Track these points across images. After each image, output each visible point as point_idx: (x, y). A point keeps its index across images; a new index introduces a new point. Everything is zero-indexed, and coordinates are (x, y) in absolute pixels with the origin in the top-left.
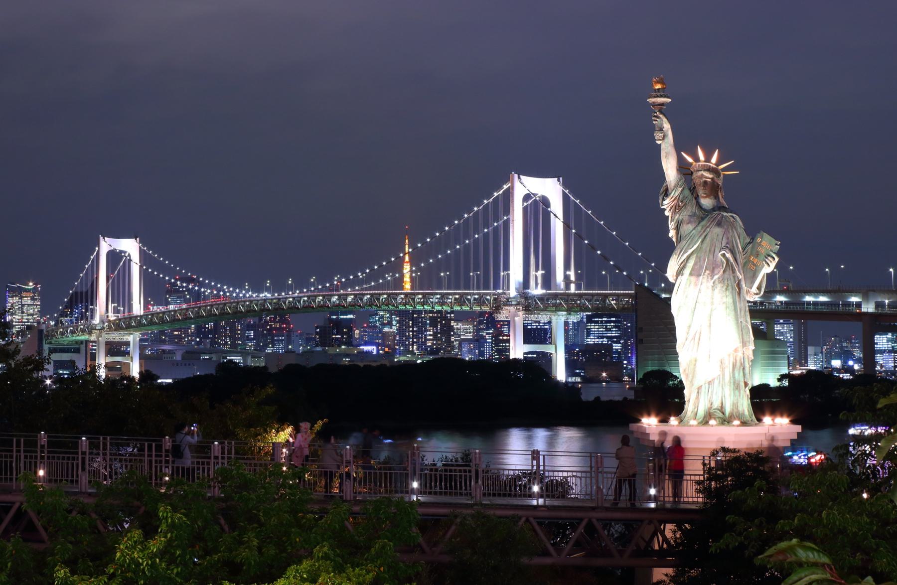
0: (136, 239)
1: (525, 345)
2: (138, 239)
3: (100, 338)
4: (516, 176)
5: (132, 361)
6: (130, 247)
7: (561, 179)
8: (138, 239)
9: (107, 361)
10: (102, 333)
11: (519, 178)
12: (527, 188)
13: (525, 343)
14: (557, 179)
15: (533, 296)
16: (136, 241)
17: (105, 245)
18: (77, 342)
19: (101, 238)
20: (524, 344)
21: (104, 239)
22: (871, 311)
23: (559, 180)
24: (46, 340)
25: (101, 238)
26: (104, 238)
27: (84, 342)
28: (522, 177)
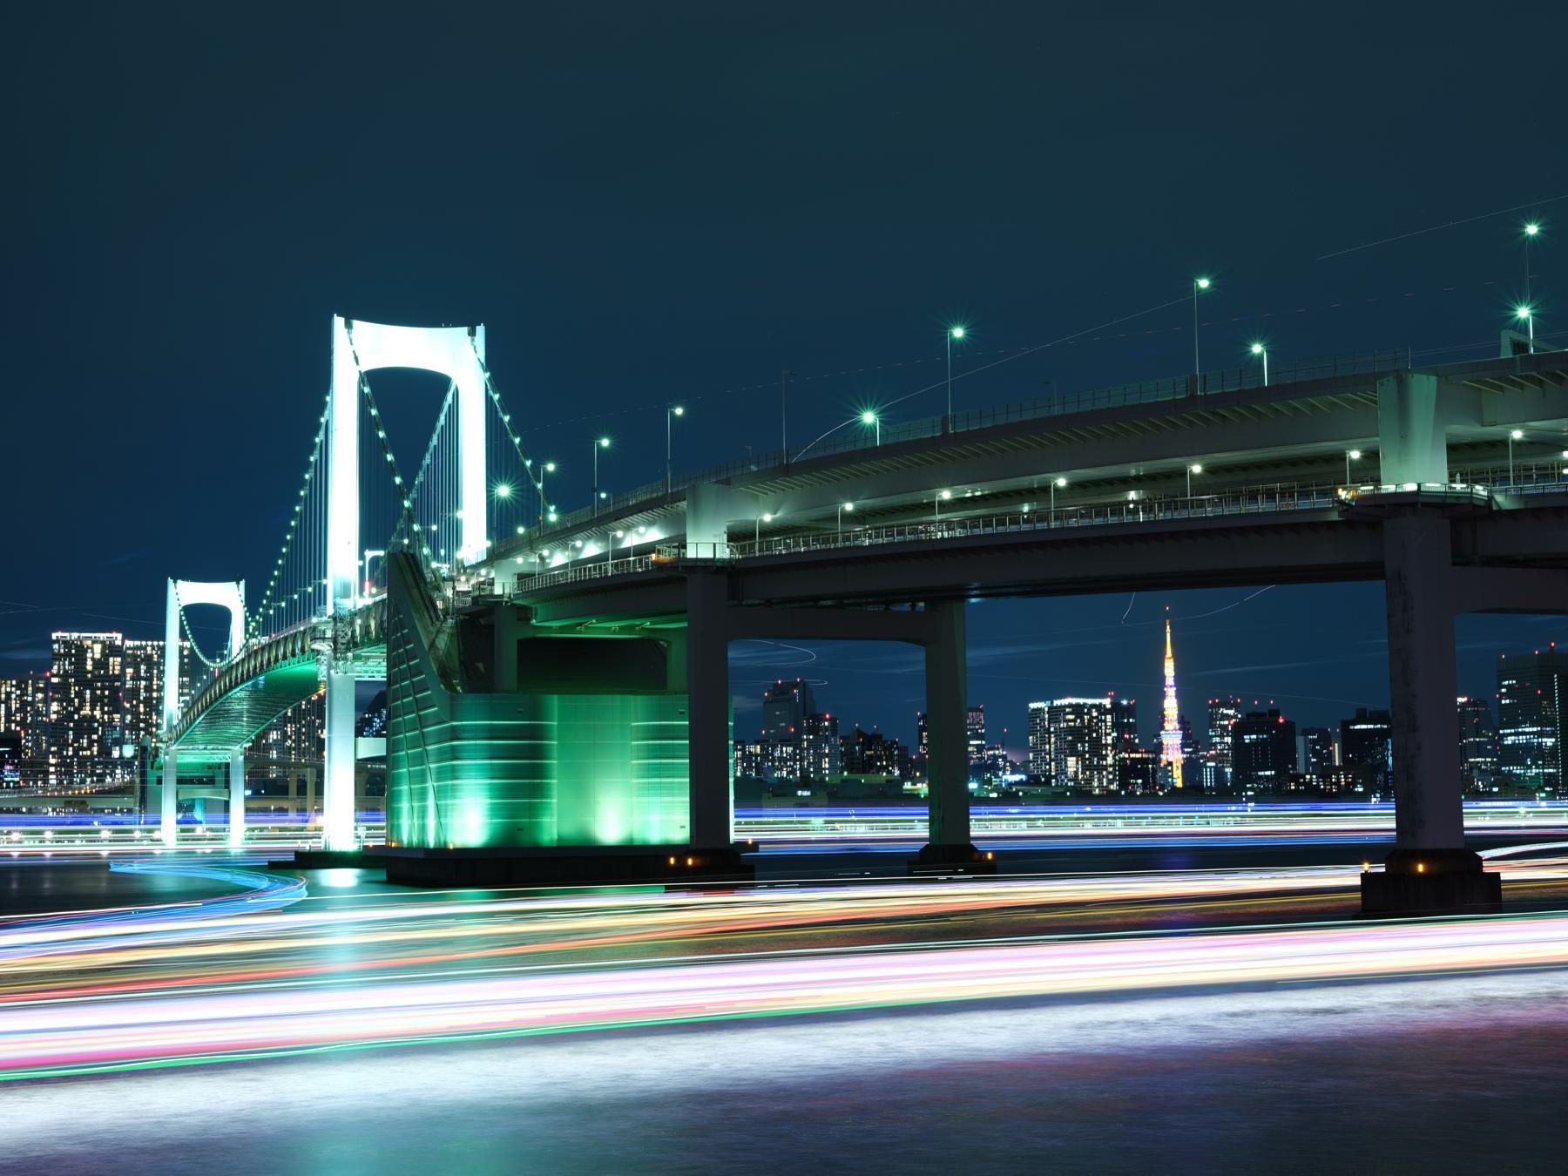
0: (238, 583)
1: (360, 739)
2: (242, 583)
3: (167, 757)
4: (339, 322)
5: (230, 797)
6: (229, 595)
7: (481, 330)
8: (242, 583)
9: (180, 798)
10: (168, 747)
11: (348, 325)
12: (355, 347)
13: (359, 732)
14: (465, 330)
15: (354, 615)
16: (238, 587)
17: (183, 593)
18: (210, 767)
19: (170, 581)
20: (356, 736)
21: (175, 582)
22: (705, 553)
23: (472, 333)
24: (152, 764)
25: (170, 581)
26: (175, 582)
27: (223, 767)
28: (355, 323)
